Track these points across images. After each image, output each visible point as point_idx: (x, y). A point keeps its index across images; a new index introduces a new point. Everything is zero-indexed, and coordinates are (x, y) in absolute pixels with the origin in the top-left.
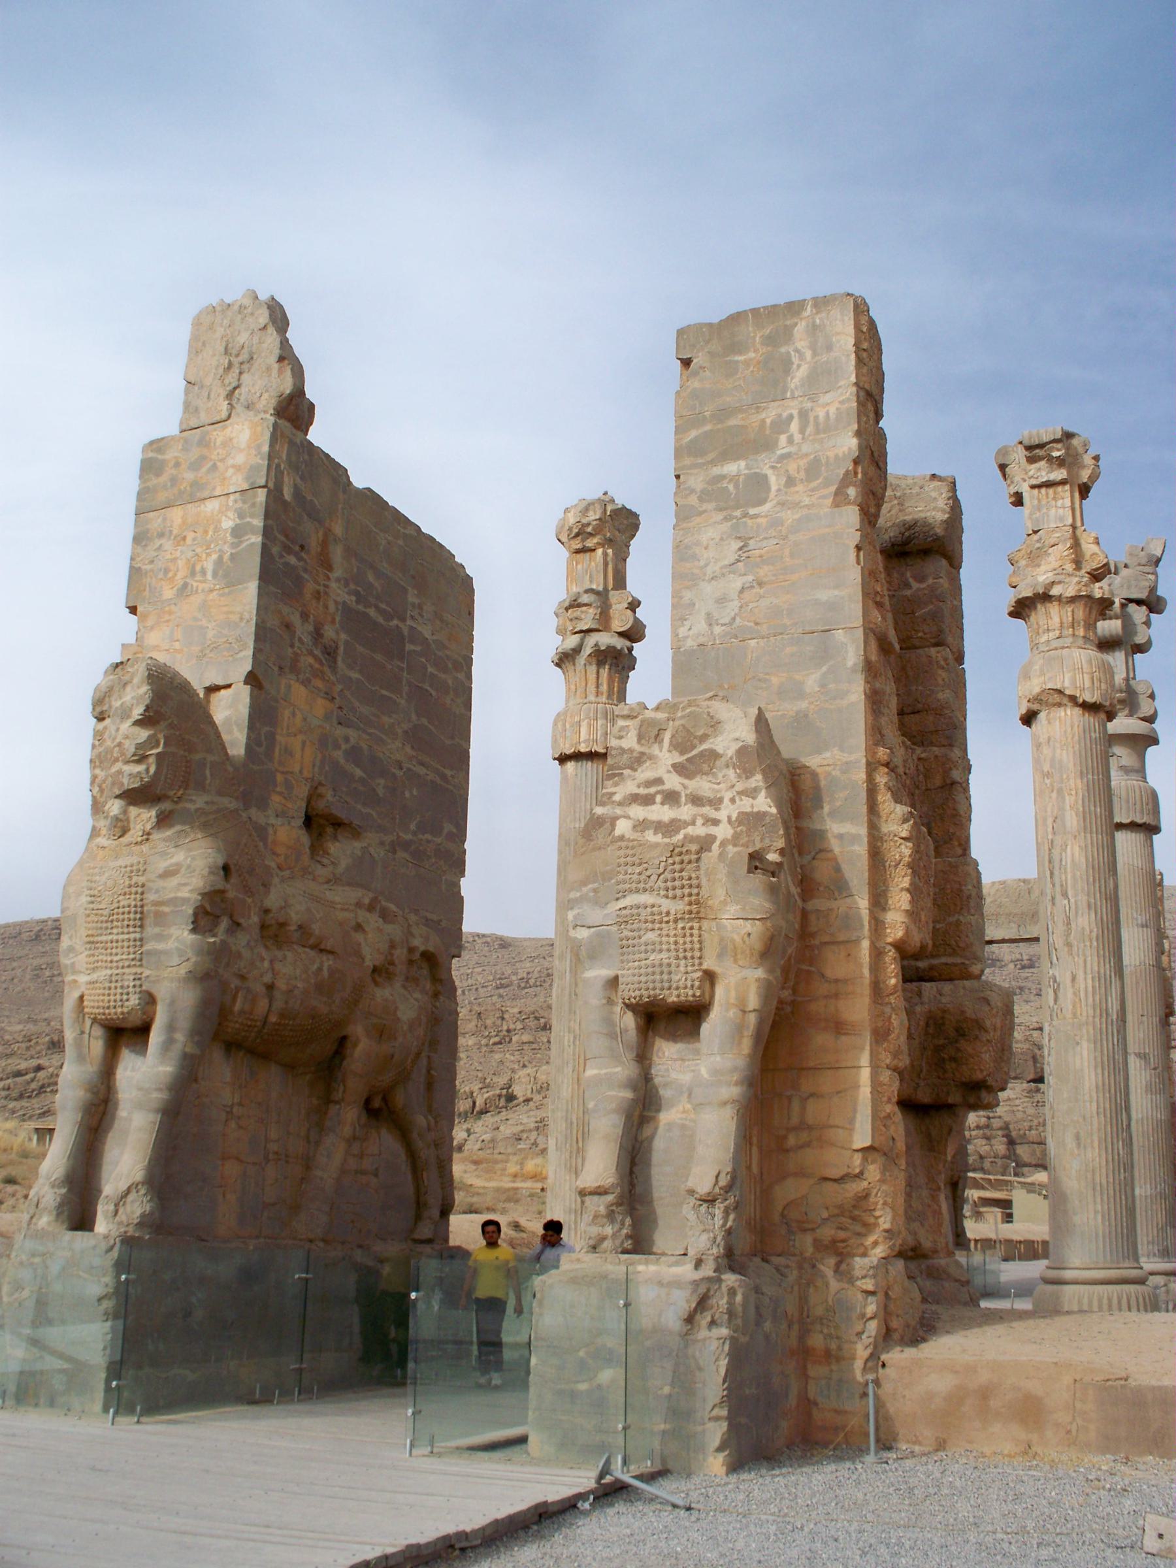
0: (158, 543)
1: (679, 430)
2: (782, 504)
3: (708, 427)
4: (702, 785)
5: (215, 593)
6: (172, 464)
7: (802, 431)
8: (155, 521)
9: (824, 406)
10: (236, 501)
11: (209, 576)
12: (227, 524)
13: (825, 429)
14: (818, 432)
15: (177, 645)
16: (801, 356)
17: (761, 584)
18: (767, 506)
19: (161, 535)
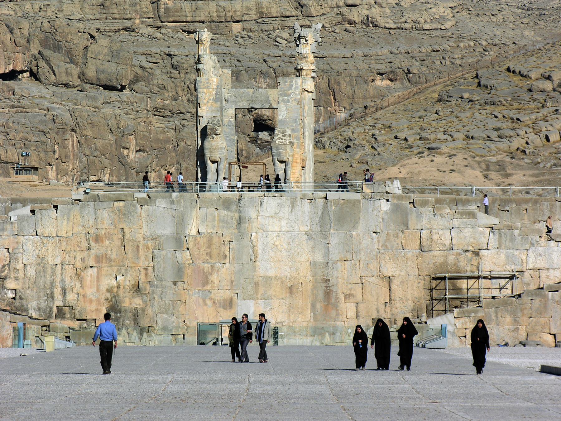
4: (285, 138)
12: (214, 93)
13: (296, 95)
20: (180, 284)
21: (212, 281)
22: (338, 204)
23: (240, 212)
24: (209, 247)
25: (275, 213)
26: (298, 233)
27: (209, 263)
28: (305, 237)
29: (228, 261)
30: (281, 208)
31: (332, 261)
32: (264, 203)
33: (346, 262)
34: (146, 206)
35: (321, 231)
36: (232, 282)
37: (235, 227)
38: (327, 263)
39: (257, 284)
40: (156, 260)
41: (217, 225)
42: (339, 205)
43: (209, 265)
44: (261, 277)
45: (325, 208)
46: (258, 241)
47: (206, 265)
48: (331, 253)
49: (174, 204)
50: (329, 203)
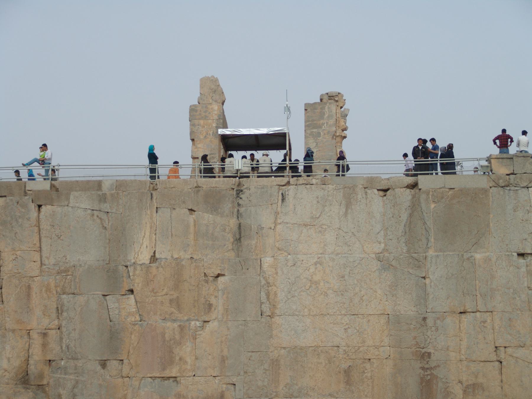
0: (198, 127)
1: (305, 122)
2: (323, 138)
3: (310, 122)
5: (213, 139)
6: (199, 110)
7: (327, 126)
8: (196, 122)
9: (330, 122)
10: (216, 121)
11: (211, 135)
14: (329, 126)
15: (205, 148)
16: (327, 113)
17: (320, 151)
18: (320, 138)
19: (198, 125)
20: (113, 365)
21: (180, 359)
22: (442, 198)
23: (239, 215)
24: (177, 287)
25: (312, 218)
26: (362, 256)
27: (175, 321)
28: (375, 265)
29: (213, 315)
30: (324, 206)
31: (434, 315)
32: (290, 198)
33: (463, 316)
34: (49, 207)
35: (408, 251)
36: (223, 360)
37: (230, 247)
38: (425, 319)
39: (275, 363)
40: (65, 314)
41: (192, 243)
42: (444, 200)
43: (176, 325)
44: (284, 348)
45: (415, 206)
46: (277, 273)
47: (169, 324)
48: (431, 297)
49: (105, 202)
50: (423, 197)
